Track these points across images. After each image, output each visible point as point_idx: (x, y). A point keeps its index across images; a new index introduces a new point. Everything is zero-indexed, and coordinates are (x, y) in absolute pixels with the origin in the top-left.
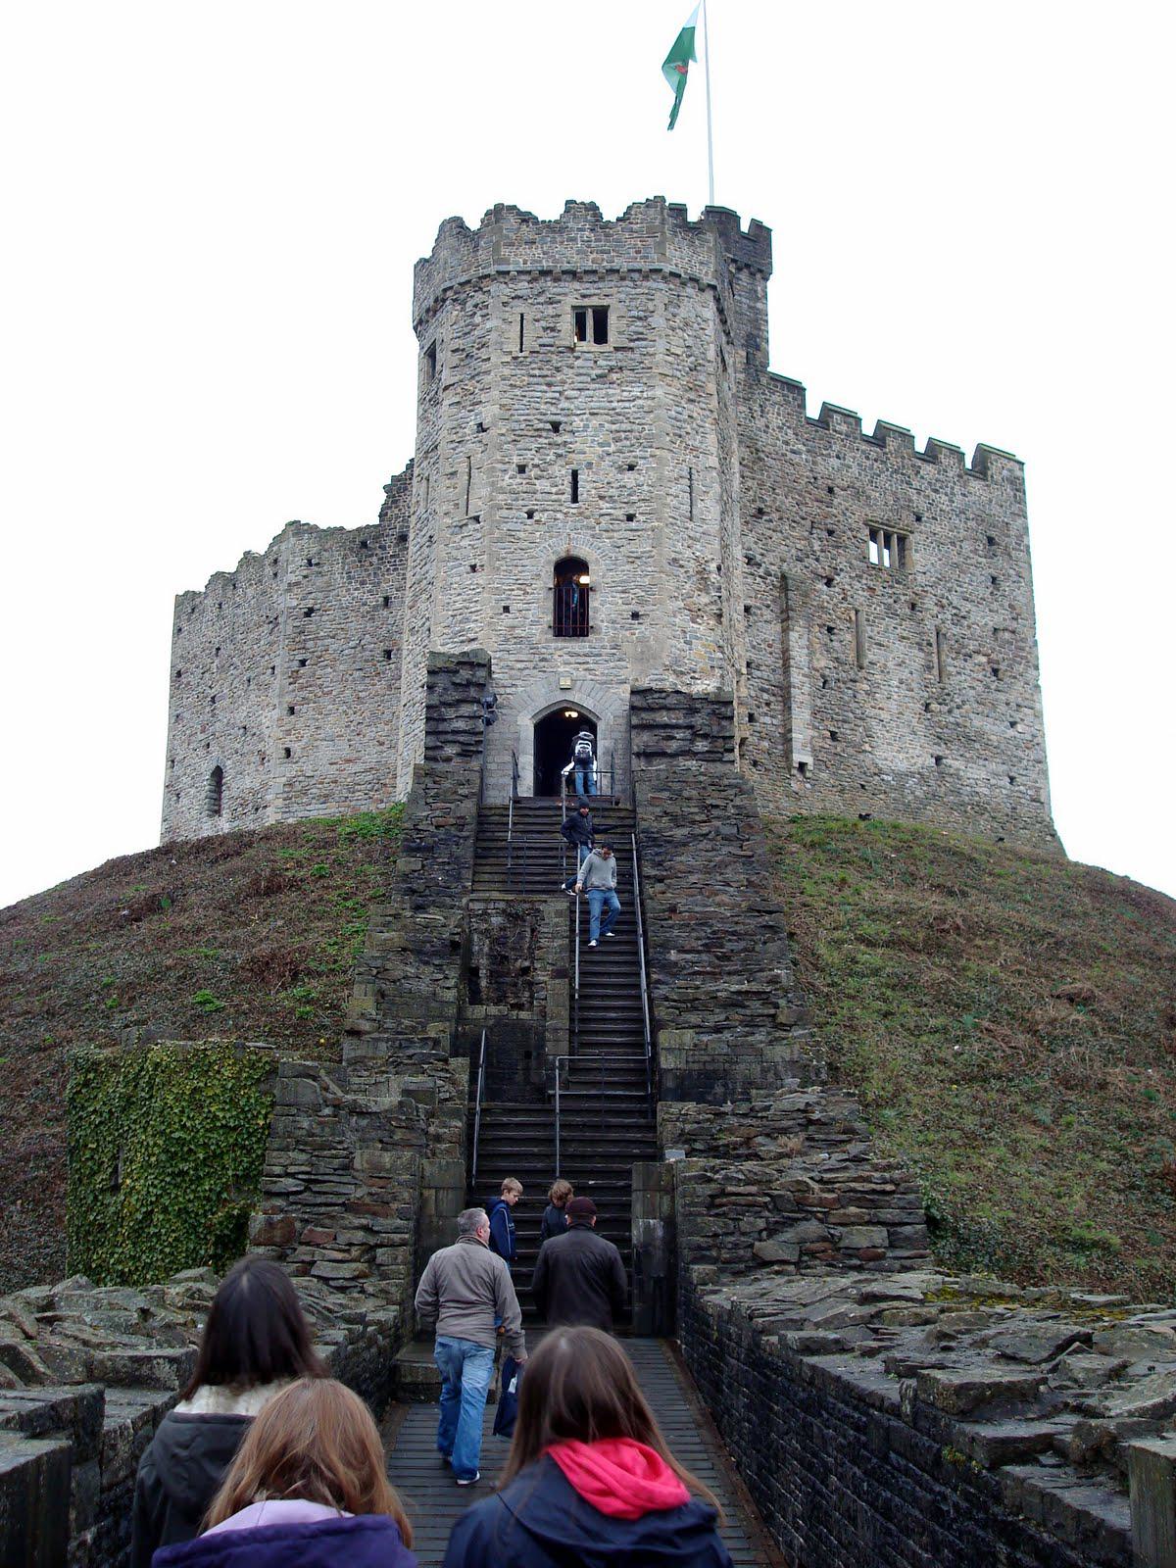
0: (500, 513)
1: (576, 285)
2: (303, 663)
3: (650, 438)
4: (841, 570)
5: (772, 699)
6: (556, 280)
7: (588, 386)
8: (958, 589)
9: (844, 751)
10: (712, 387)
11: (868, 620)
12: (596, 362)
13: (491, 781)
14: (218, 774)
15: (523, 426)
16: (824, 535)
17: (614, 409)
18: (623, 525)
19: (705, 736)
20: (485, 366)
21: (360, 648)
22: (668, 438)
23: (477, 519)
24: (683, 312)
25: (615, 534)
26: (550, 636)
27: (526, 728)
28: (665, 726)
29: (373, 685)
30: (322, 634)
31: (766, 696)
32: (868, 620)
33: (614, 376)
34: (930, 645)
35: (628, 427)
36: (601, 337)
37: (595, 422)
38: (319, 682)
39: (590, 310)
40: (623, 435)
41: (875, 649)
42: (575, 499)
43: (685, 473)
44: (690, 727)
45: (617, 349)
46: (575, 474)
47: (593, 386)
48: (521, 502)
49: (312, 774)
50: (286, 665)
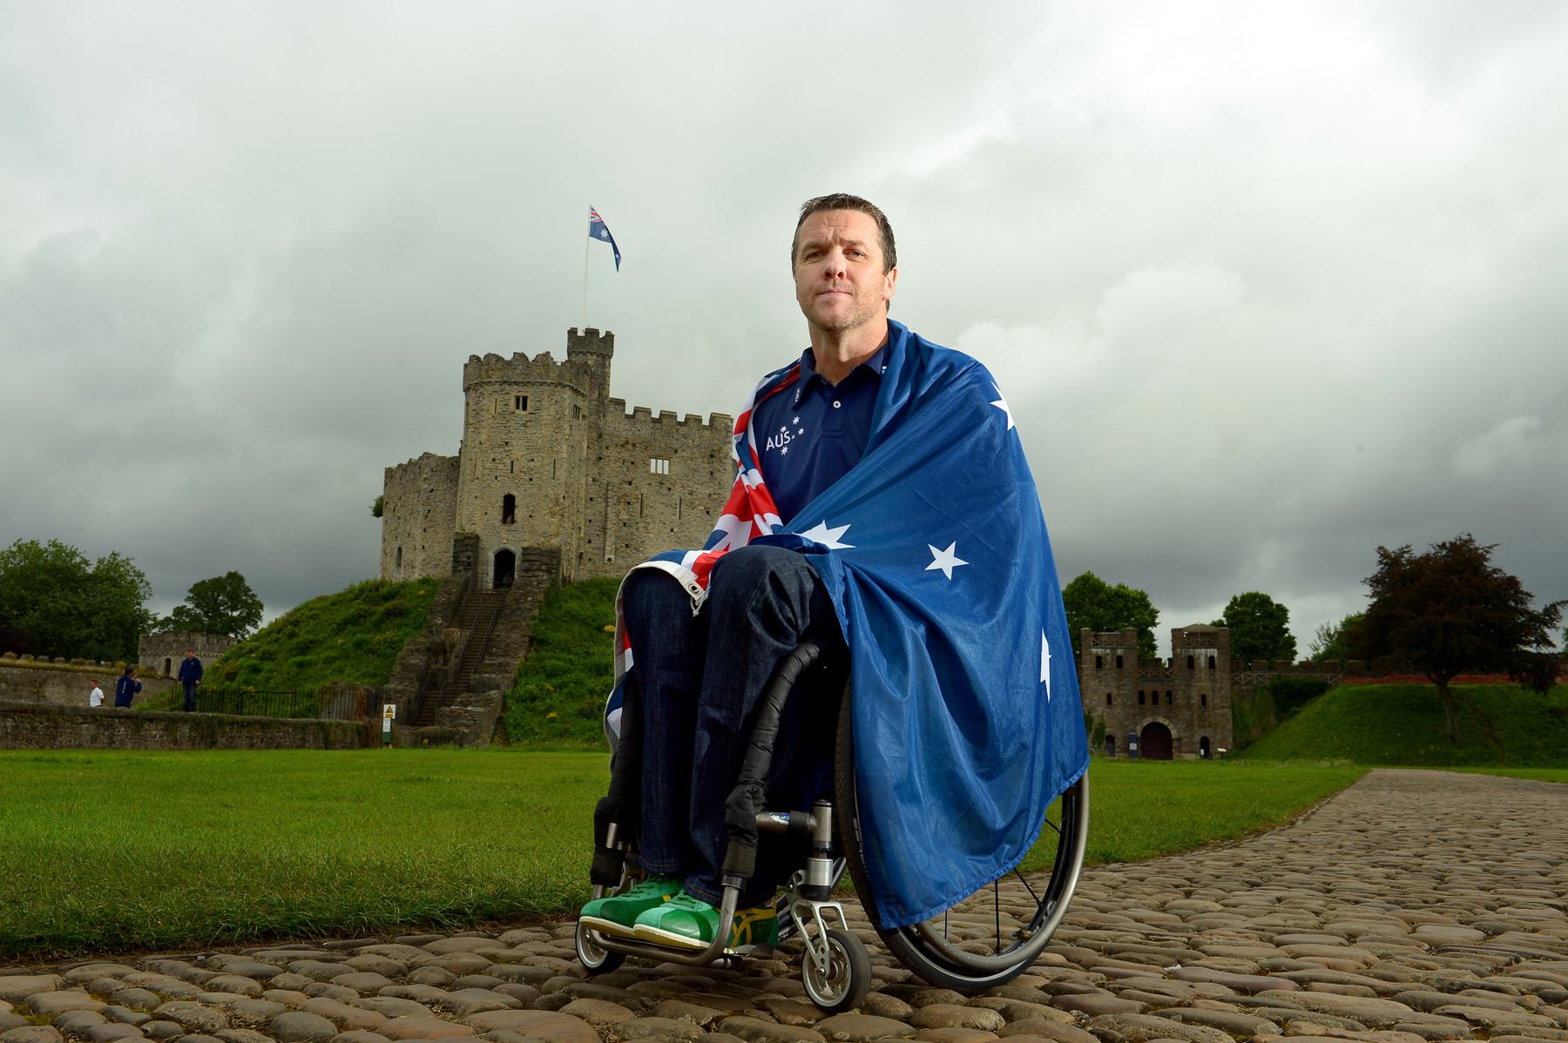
1: (516, 387)
2: (429, 511)
10: (566, 426)
14: (400, 550)
19: (546, 564)
27: (491, 556)
28: (533, 561)
33: (528, 424)
35: (531, 444)
36: (525, 408)
39: (521, 398)
41: (649, 509)
42: (512, 473)
46: (512, 462)
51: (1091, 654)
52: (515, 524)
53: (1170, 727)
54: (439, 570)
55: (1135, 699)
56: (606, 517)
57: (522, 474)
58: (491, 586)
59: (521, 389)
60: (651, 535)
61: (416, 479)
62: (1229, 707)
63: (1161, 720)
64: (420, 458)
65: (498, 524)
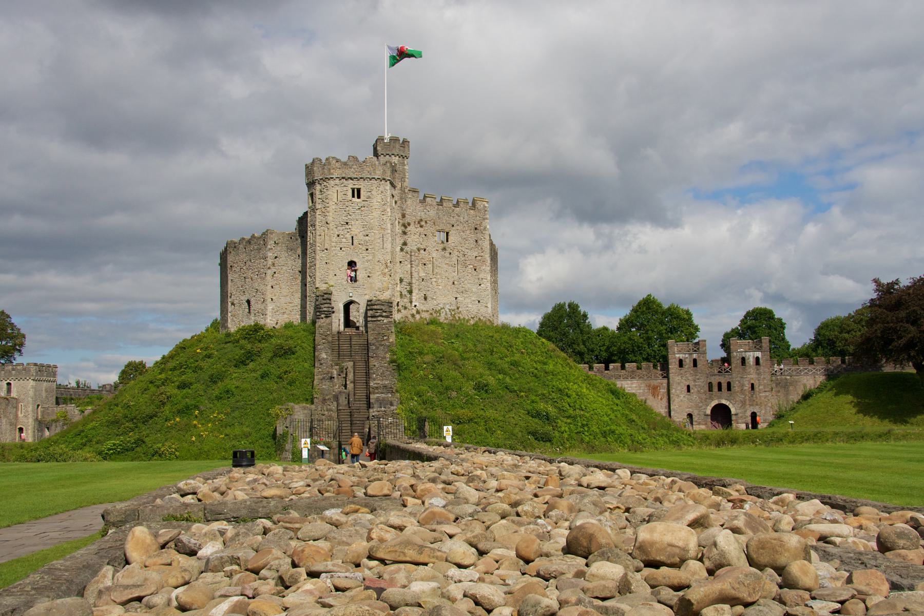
1: (352, 181)
2: (275, 273)
6: (346, 180)
10: (389, 210)
14: (248, 302)
19: (386, 312)
24: (380, 189)
33: (362, 209)
35: (366, 223)
36: (359, 197)
37: (357, 222)
39: (356, 190)
46: (352, 237)
51: (675, 358)
53: (731, 406)
54: (285, 316)
55: (707, 388)
56: (411, 275)
58: (342, 328)
59: (355, 182)
60: (440, 287)
61: (260, 249)
62: (768, 391)
63: (724, 402)
64: (264, 234)
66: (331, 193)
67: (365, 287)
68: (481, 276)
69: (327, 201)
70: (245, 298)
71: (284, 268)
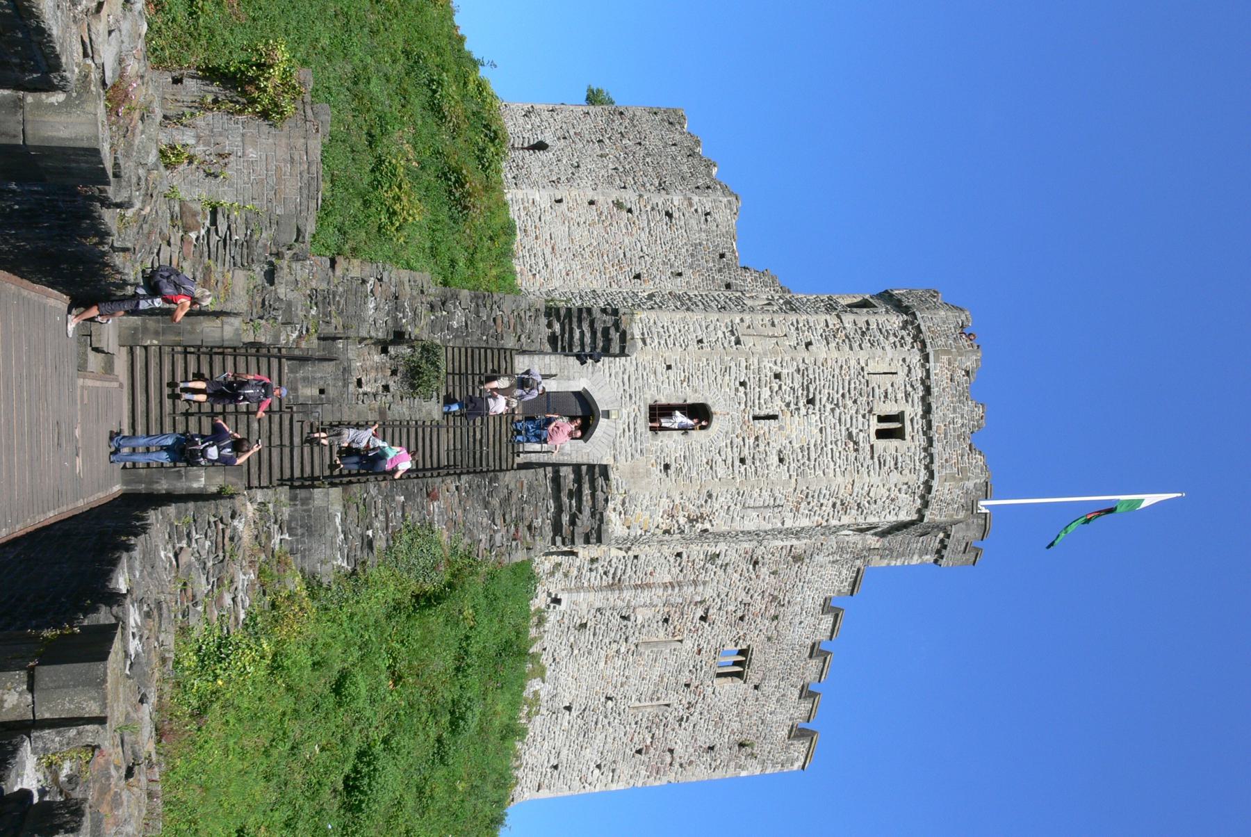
0: (743, 360)
1: (920, 413)
2: (630, 211)
3: (803, 474)
4: (713, 628)
5: (610, 576)
6: (923, 399)
7: (843, 425)
8: (703, 720)
9: (572, 634)
10: (846, 520)
11: (675, 650)
12: (861, 431)
13: (536, 358)
14: (541, 146)
15: (811, 376)
16: (739, 614)
17: (826, 445)
18: (737, 454)
19: (573, 522)
20: (856, 346)
21: (641, 254)
22: (805, 488)
23: (738, 342)
25: (729, 449)
26: (650, 402)
29: (613, 266)
30: (652, 225)
31: (612, 571)
32: (675, 650)
33: (851, 445)
34: (658, 699)
35: (813, 456)
36: (881, 434)
38: (615, 224)
39: (900, 425)
40: (806, 453)
42: (755, 418)
43: (778, 502)
44: (581, 513)
45: (872, 447)
46: (774, 417)
47: (843, 428)
48: (752, 376)
49: (543, 221)
50: (627, 198)
52: (650, 433)
57: (752, 440)
59: (919, 424)
60: (602, 664)
65: (648, 396)
66: (890, 356)
67: (637, 456)
68: (624, 769)
69: (866, 345)
70: (548, 138)
71: (644, 236)
